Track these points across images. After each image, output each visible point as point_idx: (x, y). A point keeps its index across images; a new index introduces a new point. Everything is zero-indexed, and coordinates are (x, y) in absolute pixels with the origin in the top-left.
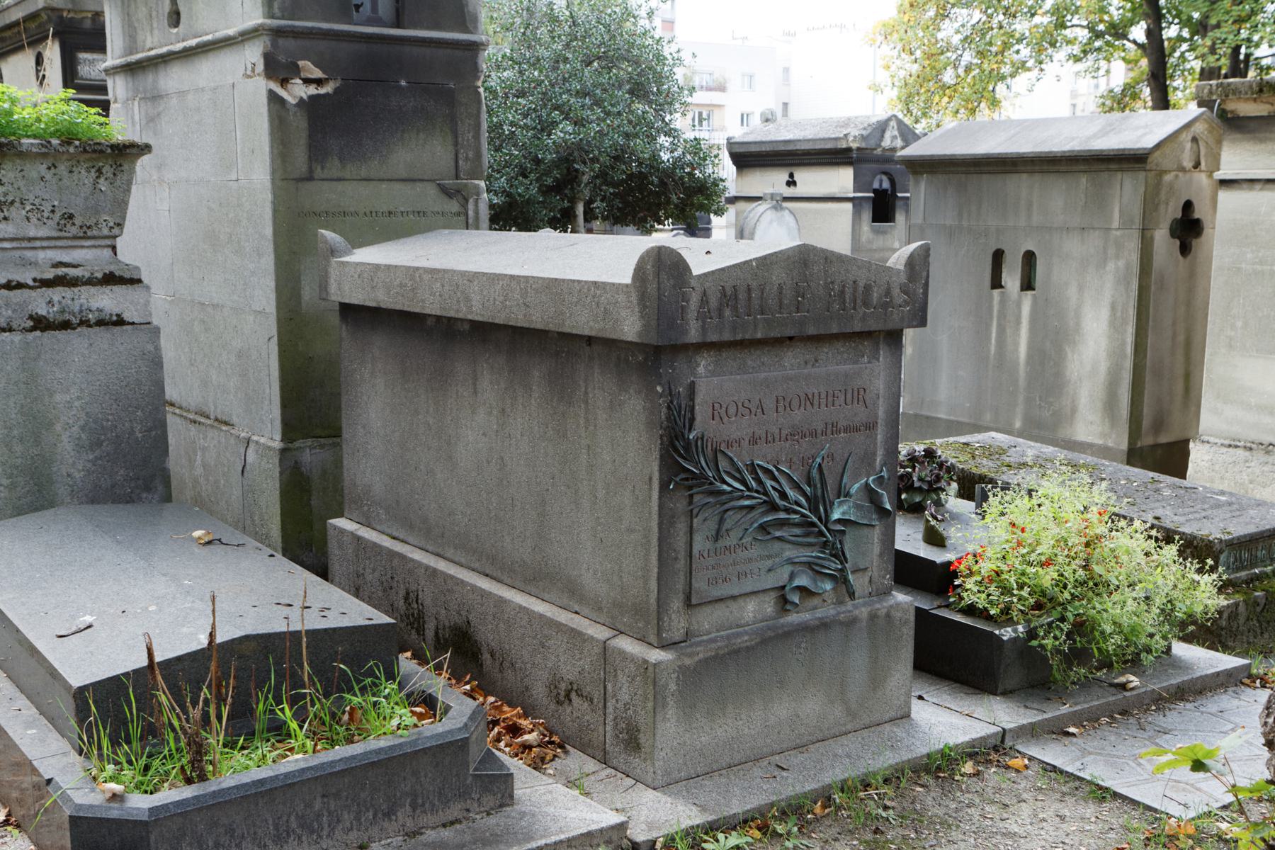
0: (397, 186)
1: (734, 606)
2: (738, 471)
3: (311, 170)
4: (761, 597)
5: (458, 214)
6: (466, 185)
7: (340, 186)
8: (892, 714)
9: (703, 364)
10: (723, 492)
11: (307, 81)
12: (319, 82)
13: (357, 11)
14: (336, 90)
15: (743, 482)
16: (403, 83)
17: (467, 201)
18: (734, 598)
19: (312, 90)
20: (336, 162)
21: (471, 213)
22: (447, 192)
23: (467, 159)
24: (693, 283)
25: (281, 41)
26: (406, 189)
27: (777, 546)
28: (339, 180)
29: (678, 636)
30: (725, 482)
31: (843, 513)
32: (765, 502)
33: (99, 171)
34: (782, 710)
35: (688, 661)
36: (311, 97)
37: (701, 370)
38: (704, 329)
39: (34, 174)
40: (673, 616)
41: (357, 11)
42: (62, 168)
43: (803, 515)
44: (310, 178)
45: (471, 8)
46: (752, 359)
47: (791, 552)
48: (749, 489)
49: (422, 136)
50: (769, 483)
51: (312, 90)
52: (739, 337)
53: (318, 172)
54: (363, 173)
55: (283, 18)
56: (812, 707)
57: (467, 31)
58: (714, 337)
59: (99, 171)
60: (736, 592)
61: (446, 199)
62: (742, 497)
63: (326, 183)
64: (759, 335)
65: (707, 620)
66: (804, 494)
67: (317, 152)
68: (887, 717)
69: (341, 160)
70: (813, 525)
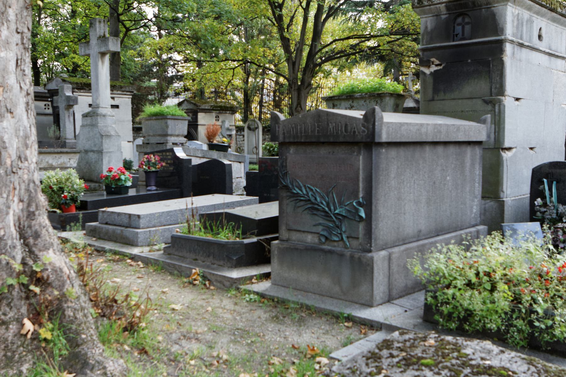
0: (465, 101)
1: (304, 235)
2: (301, 187)
3: (433, 97)
4: (313, 235)
6: (494, 99)
7: (443, 102)
8: (363, 302)
9: (292, 150)
11: (437, 65)
12: (440, 65)
14: (443, 67)
15: (302, 191)
16: (469, 61)
17: (494, 105)
18: (304, 232)
19: (439, 68)
20: (443, 94)
21: (497, 110)
22: (486, 102)
23: (496, 88)
24: (281, 123)
25: (425, 53)
26: (469, 102)
27: (317, 218)
28: (443, 100)
29: (285, 238)
31: (340, 212)
33: (377, 102)
34: (314, 278)
35: (281, 246)
36: (435, 71)
37: (291, 152)
38: (284, 138)
39: (361, 104)
42: (368, 101)
44: (433, 100)
45: (500, 26)
46: (309, 149)
47: (321, 221)
49: (476, 80)
50: (310, 193)
51: (436, 68)
52: (296, 141)
53: (436, 98)
54: (452, 97)
55: (427, 45)
56: (326, 282)
57: (498, 35)
58: (287, 140)
59: (377, 102)
60: (302, 229)
61: (486, 105)
63: (439, 102)
64: (303, 141)
65: (295, 236)
66: (325, 201)
67: (436, 91)
68: (360, 302)
69: (444, 92)
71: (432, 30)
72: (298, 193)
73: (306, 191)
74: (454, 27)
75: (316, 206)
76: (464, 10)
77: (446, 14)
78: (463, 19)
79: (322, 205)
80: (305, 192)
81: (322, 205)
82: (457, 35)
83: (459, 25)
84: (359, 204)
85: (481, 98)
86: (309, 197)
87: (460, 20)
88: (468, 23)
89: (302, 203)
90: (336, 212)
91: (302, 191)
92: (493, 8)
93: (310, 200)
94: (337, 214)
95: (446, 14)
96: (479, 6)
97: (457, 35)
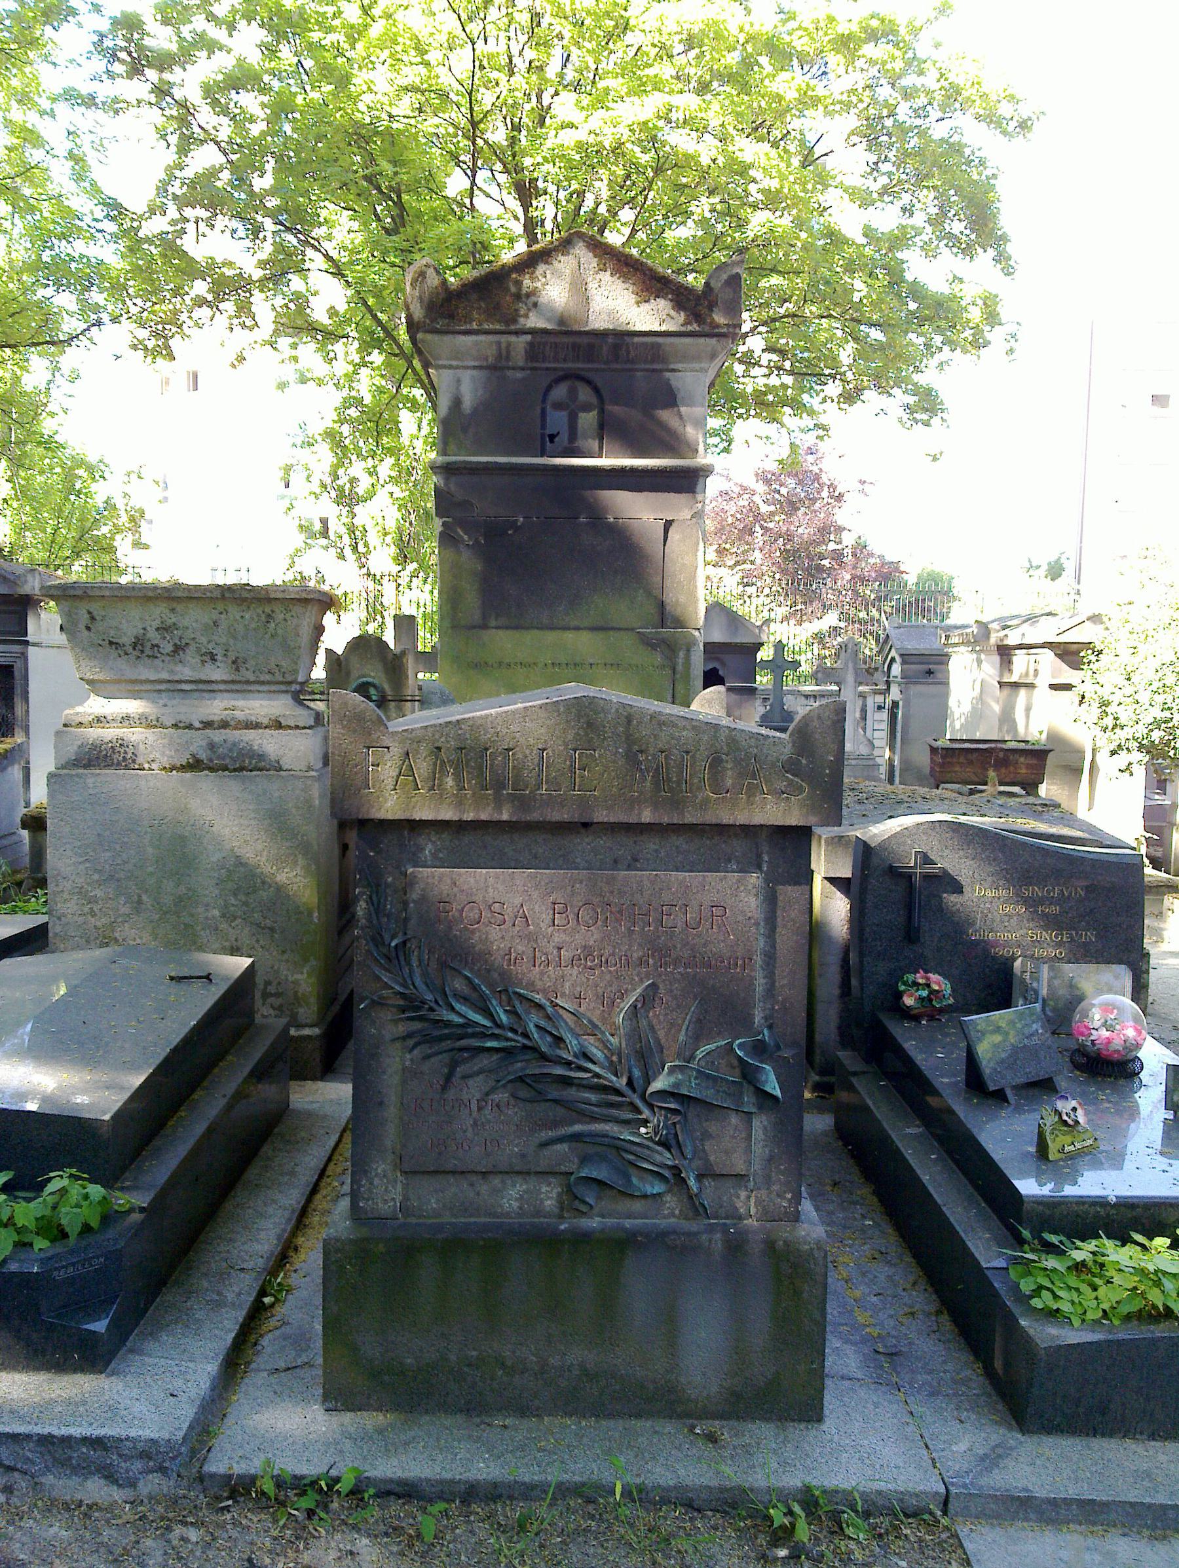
2: (483, 997)
5: (663, 667)
10: (448, 1024)
13: (552, 441)
15: (490, 1015)
30: (453, 1009)
31: (677, 1085)
32: (525, 1047)
40: (376, 1181)
41: (552, 441)
43: (597, 1076)
48: (499, 1025)
50: (533, 1020)
52: (469, 816)
62: (484, 1036)
70: (618, 1092)
71: (475, 410)
72: (470, 1023)
73: (513, 1013)
74: (543, 413)
75: (559, 1071)
76: (580, 365)
77: (523, 369)
78: (573, 392)
79: (590, 1066)
80: (504, 1018)
81: (590, 1066)
82: (552, 438)
83: (558, 406)
84: (759, 1049)
85: (633, 629)
86: (526, 1035)
87: (560, 392)
88: (586, 408)
89: (485, 1061)
90: (658, 1085)
91: (490, 1015)
92: (668, 374)
93: (535, 1049)
94: (662, 1094)
95: (523, 369)
96: (628, 361)
97: (552, 438)
